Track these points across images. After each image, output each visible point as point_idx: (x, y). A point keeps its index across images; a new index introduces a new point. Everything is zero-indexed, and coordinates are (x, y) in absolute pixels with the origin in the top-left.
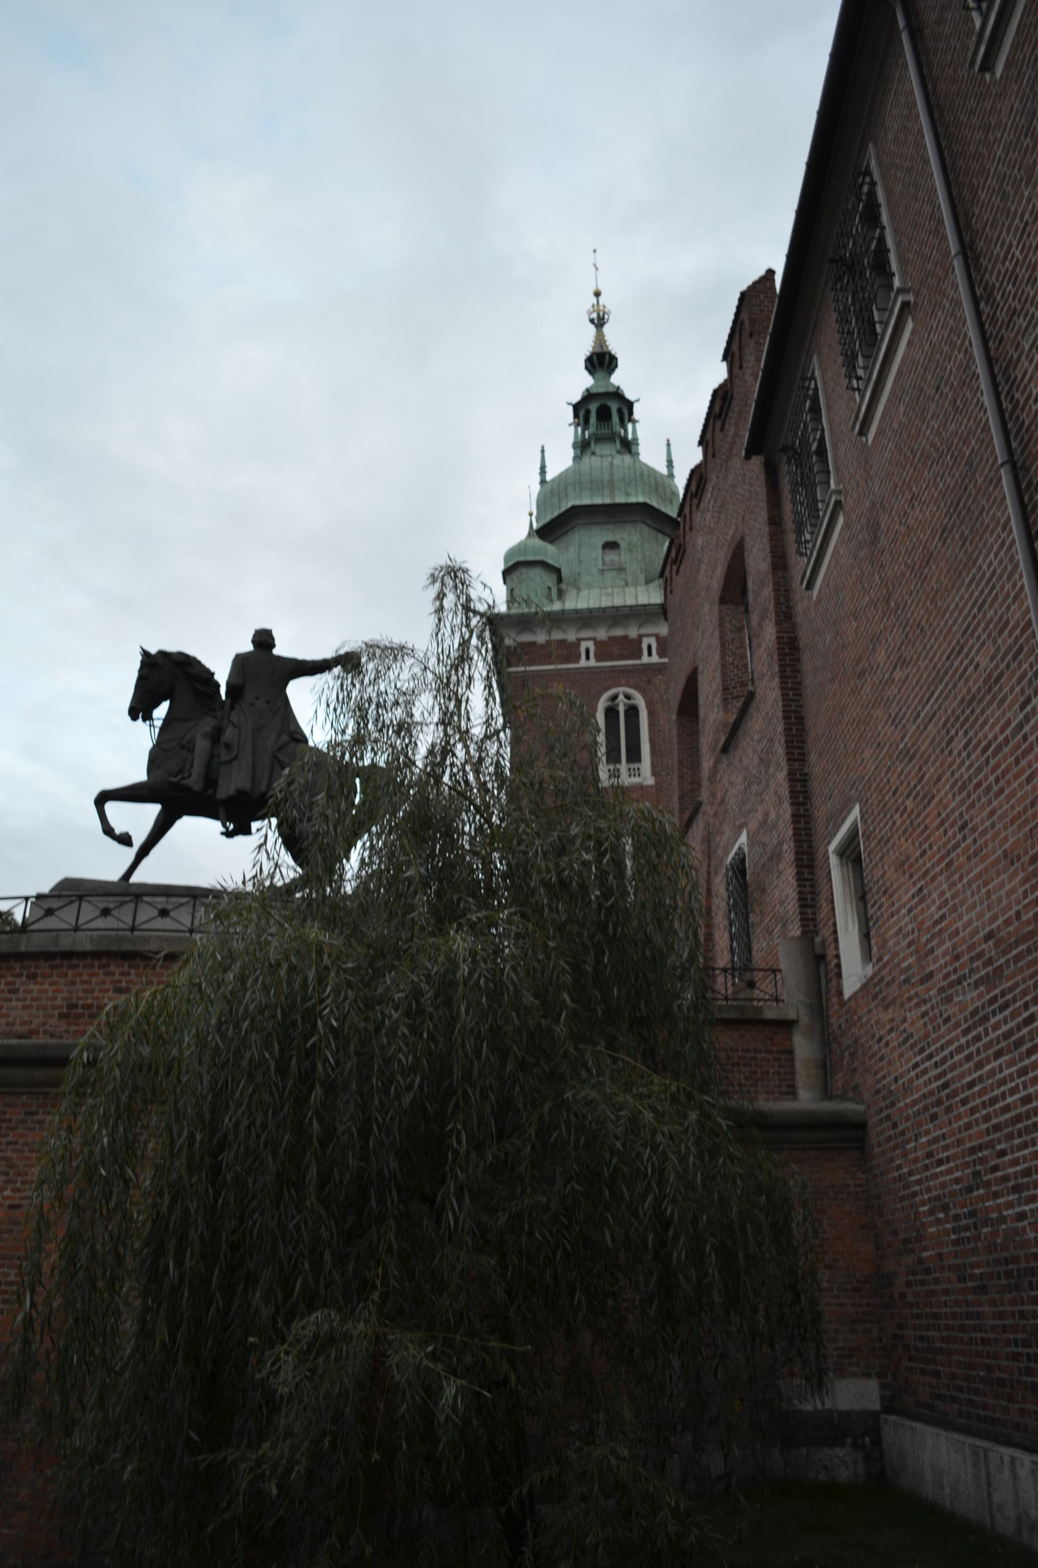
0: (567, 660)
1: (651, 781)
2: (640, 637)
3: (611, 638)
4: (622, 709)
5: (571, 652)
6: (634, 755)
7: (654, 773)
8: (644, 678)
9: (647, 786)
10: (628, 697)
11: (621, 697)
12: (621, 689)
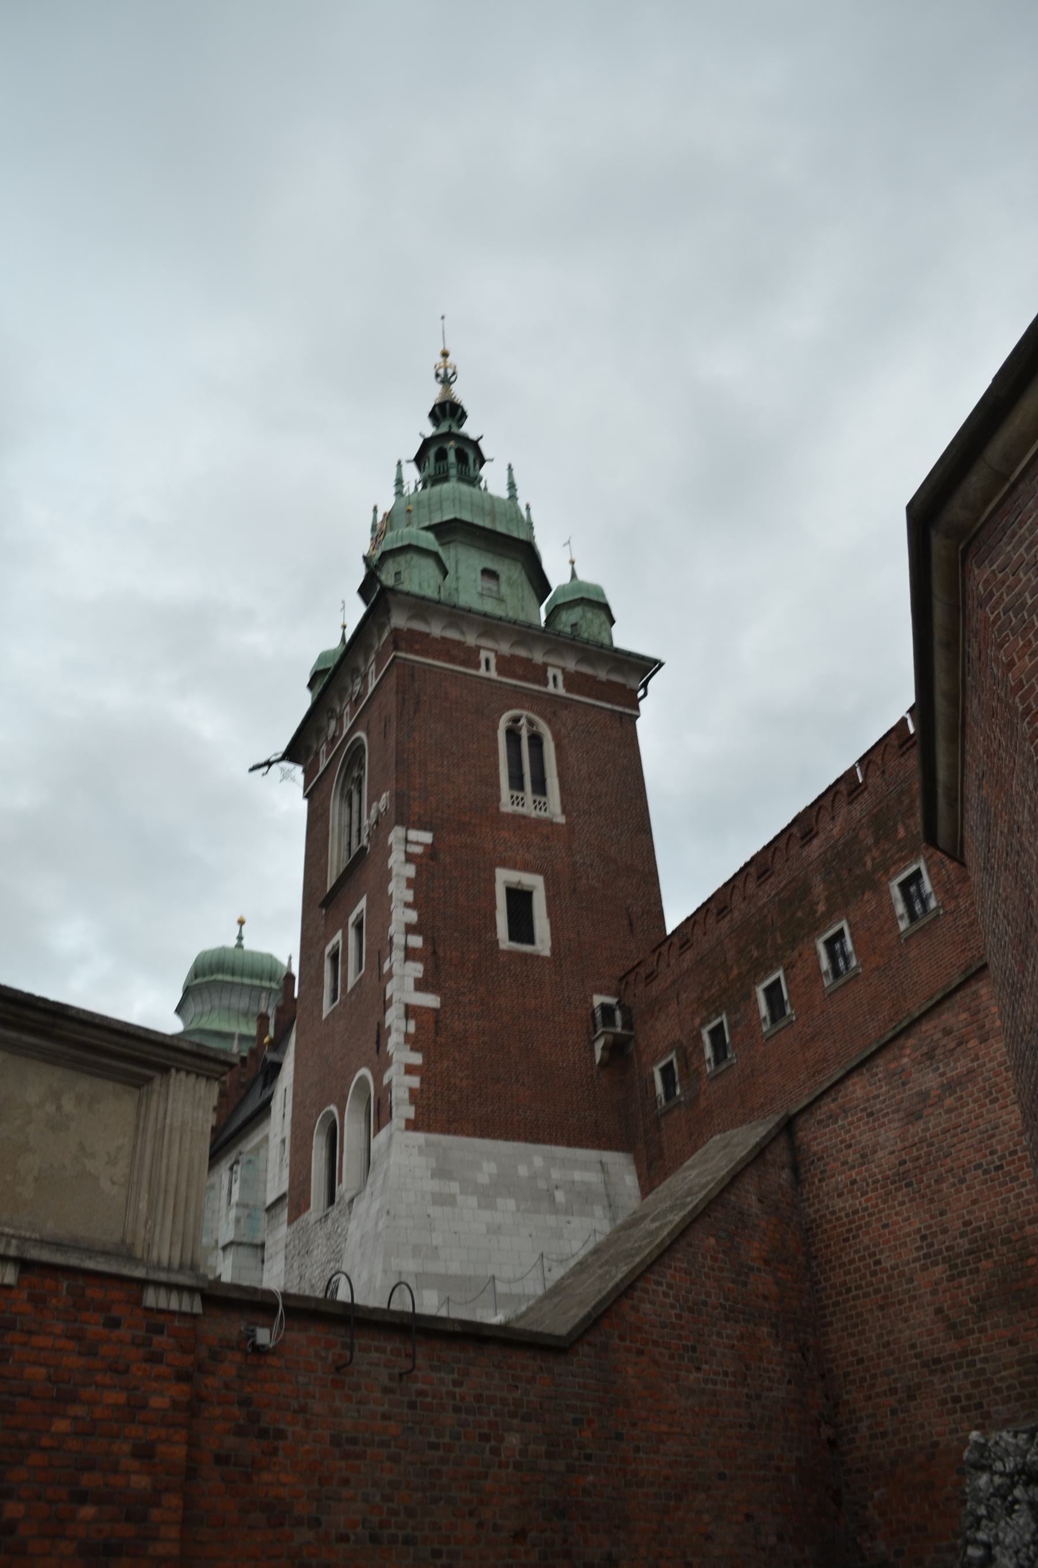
1: (561, 819)
3: (513, 656)
4: (524, 734)
5: (470, 657)
6: (540, 787)
7: (564, 811)
9: (557, 824)
12: (525, 713)
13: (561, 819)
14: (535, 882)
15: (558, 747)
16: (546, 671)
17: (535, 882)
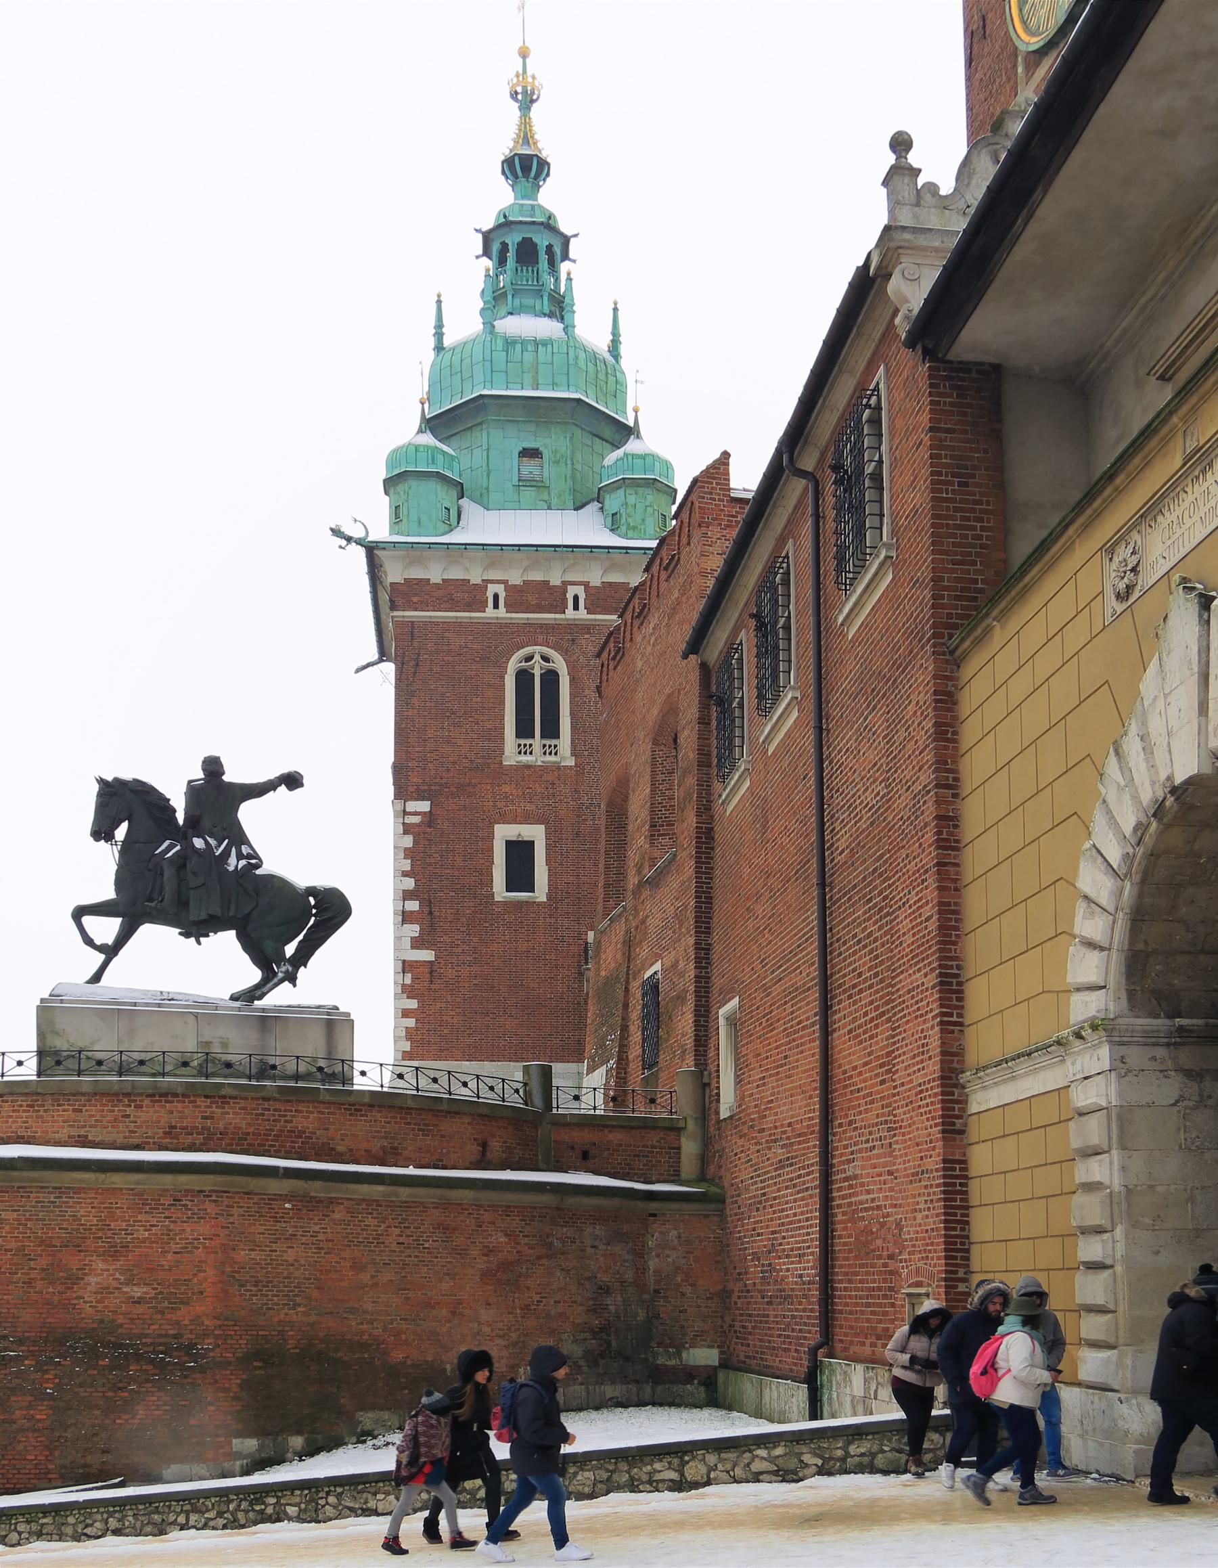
0: (469, 607)
1: (571, 762)
2: (565, 584)
6: (551, 730)
7: (574, 753)
8: (564, 637)
10: (545, 659)
11: (537, 657)
13: (571, 762)
14: (536, 833)
15: (573, 680)
16: (565, 592)
17: (536, 833)
